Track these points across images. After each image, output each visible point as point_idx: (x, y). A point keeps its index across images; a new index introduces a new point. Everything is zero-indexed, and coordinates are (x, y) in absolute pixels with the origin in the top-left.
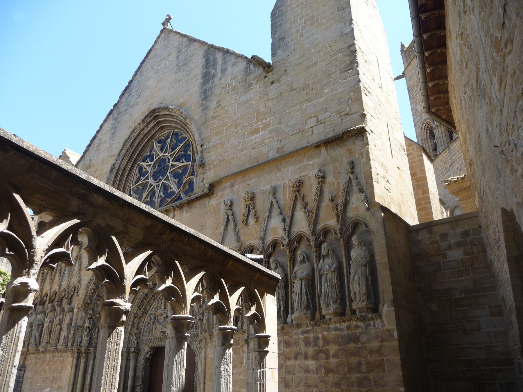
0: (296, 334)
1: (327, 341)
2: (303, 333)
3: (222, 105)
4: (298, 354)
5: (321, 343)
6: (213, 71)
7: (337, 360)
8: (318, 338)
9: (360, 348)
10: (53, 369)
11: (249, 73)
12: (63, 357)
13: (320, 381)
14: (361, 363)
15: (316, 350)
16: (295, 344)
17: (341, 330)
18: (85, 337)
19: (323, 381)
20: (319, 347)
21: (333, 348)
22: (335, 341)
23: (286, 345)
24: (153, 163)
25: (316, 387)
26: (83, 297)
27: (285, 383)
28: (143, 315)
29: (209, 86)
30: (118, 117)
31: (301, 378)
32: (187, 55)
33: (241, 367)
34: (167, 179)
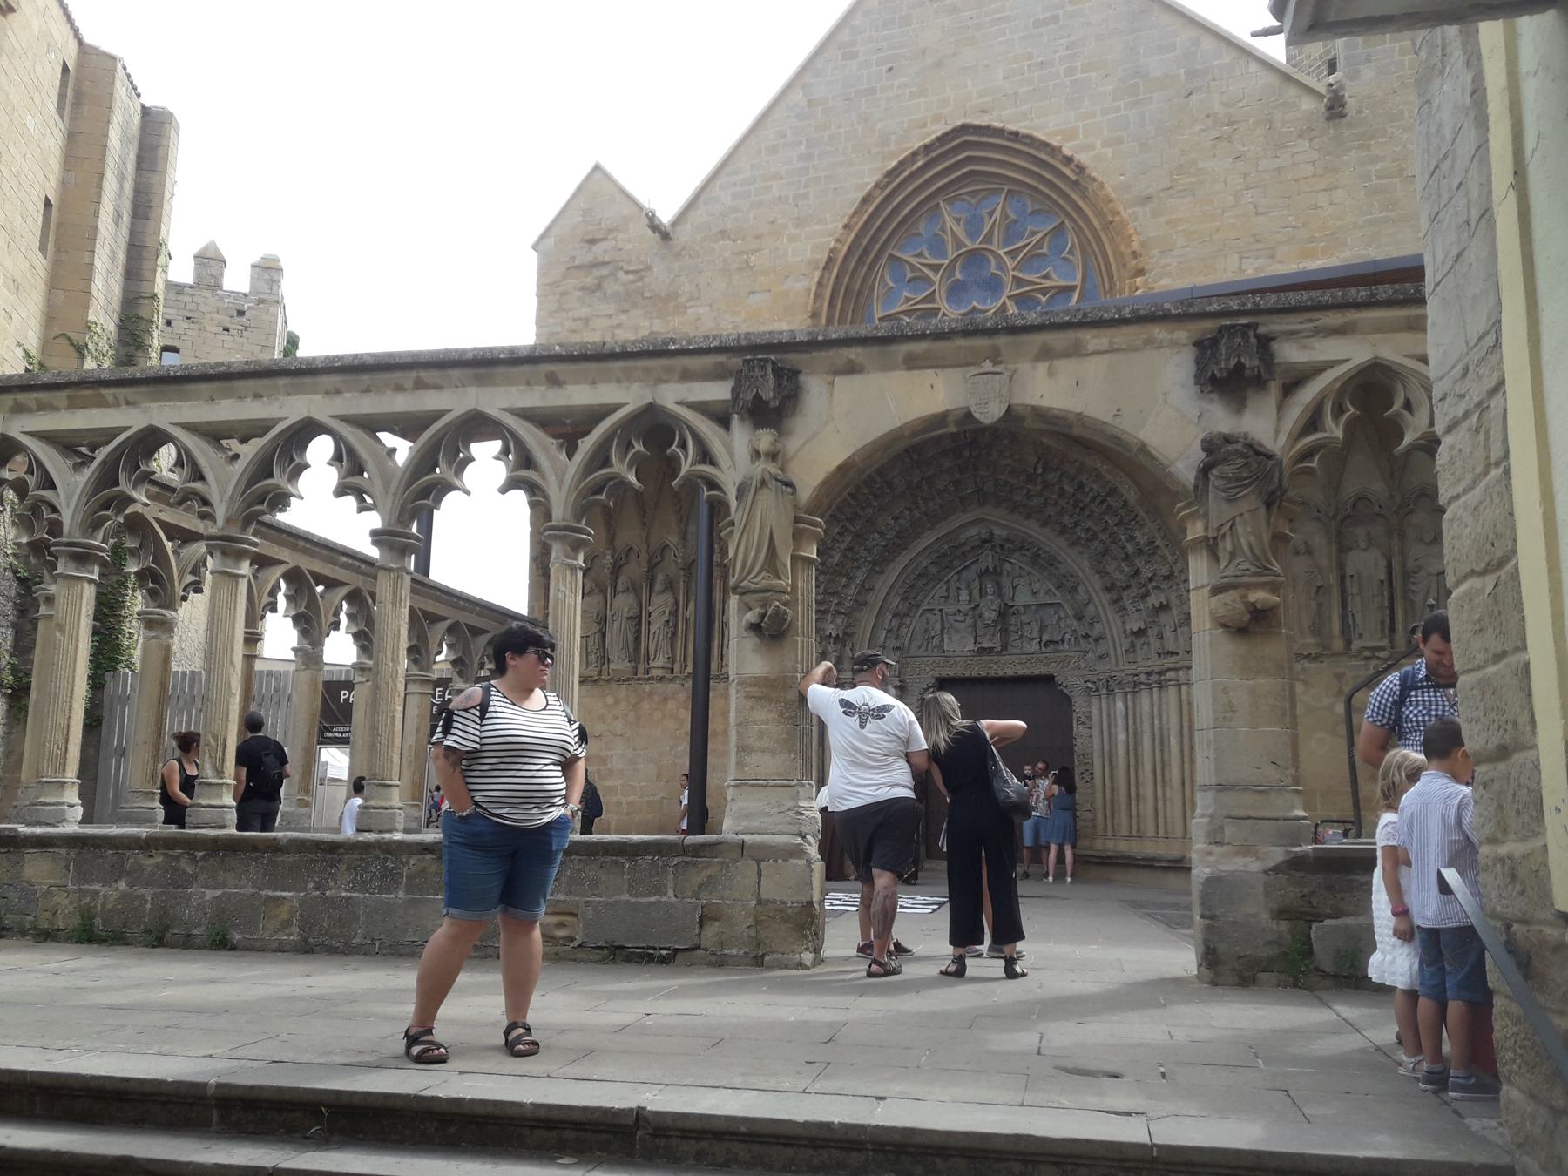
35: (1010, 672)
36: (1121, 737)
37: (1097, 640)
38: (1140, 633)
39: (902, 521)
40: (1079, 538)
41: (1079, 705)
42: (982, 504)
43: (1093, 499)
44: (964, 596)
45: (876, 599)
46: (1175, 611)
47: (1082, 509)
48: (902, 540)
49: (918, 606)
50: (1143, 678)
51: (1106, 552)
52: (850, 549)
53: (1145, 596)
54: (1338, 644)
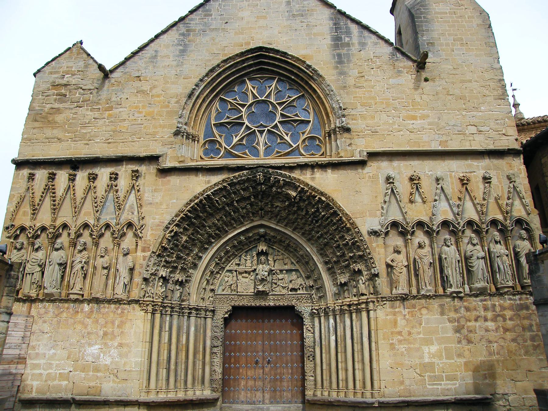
0: (475, 301)
1: (503, 308)
2: (481, 301)
3: (366, 77)
4: (479, 317)
5: (498, 309)
6: (347, 39)
7: (513, 322)
8: (495, 305)
9: (531, 314)
10: (102, 321)
11: (397, 60)
12: (123, 309)
13: (500, 338)
14: (533, 325)
15: (494, 315)
16: (475, 309)
17: (515, 300)
18: (160, 288)
19: (503, 338)
20: (497, 312)
21: (508, 314)
22: (511, 308)
23: (466, 309)
24: (249, 104)
25: (496, 342)
26: (160, 240)
27: (467, 340)
28: (220, 270)
29: (344, 51)
30: (189, 35)
31: (482, 336)
32: (303, 7)
33: (420, 327)
34: (276, 126)
35: (272, 304)
36: (333, 338)
37: (318, 289)
38: (343, 285)
39: (221, 222)
40: (313, 236)
41: (307, 321)
42: (262, 218)
43: (324, 216)
44: (249, 263)
45: (202, 264)
46: (365, 273)
47: (317, 222)
48: (221, 232)
49: (224, 268)
50: (346, 308)
51: (326, 244)
52: (192, 234)
53: (348, 266)
54: (441, 291)
